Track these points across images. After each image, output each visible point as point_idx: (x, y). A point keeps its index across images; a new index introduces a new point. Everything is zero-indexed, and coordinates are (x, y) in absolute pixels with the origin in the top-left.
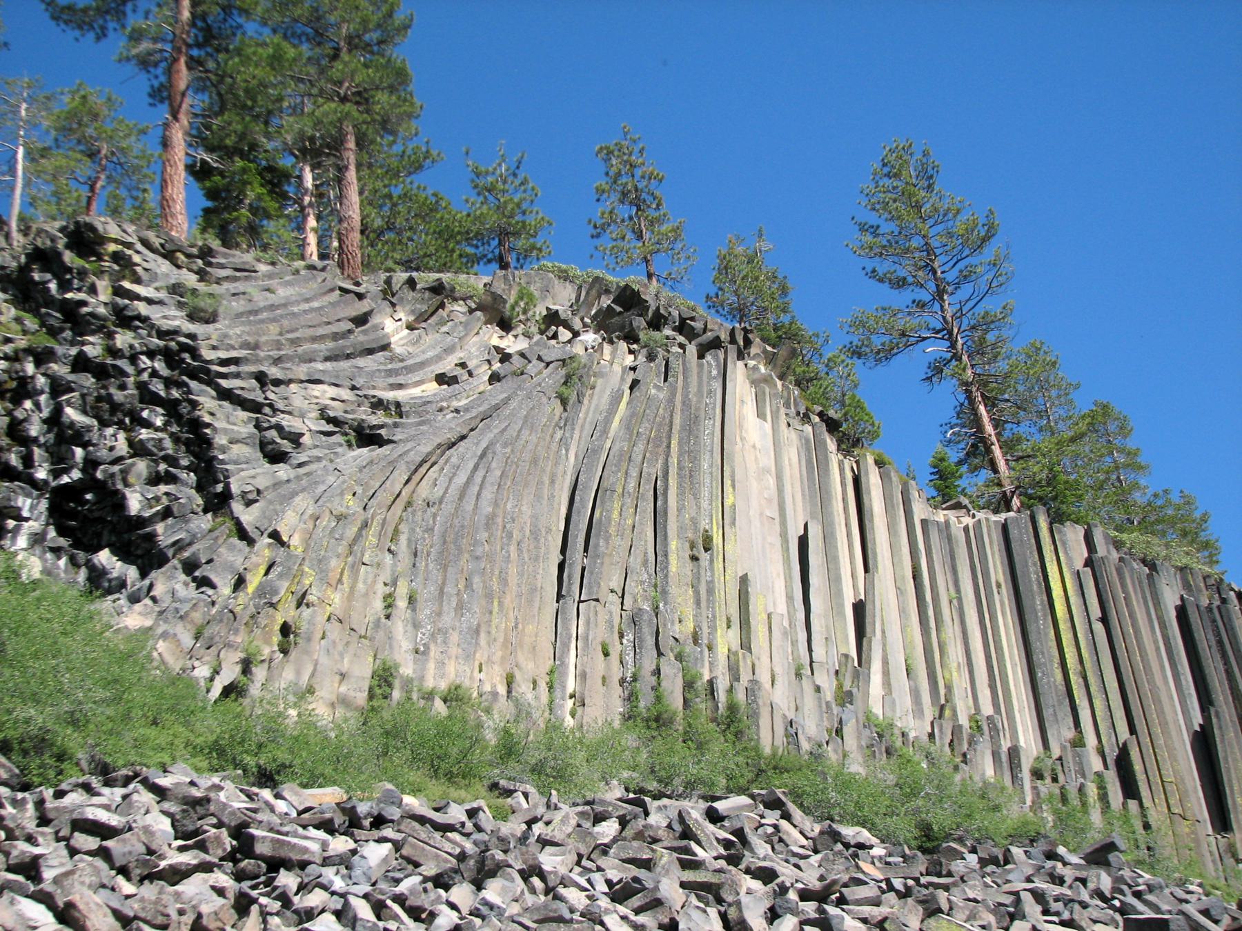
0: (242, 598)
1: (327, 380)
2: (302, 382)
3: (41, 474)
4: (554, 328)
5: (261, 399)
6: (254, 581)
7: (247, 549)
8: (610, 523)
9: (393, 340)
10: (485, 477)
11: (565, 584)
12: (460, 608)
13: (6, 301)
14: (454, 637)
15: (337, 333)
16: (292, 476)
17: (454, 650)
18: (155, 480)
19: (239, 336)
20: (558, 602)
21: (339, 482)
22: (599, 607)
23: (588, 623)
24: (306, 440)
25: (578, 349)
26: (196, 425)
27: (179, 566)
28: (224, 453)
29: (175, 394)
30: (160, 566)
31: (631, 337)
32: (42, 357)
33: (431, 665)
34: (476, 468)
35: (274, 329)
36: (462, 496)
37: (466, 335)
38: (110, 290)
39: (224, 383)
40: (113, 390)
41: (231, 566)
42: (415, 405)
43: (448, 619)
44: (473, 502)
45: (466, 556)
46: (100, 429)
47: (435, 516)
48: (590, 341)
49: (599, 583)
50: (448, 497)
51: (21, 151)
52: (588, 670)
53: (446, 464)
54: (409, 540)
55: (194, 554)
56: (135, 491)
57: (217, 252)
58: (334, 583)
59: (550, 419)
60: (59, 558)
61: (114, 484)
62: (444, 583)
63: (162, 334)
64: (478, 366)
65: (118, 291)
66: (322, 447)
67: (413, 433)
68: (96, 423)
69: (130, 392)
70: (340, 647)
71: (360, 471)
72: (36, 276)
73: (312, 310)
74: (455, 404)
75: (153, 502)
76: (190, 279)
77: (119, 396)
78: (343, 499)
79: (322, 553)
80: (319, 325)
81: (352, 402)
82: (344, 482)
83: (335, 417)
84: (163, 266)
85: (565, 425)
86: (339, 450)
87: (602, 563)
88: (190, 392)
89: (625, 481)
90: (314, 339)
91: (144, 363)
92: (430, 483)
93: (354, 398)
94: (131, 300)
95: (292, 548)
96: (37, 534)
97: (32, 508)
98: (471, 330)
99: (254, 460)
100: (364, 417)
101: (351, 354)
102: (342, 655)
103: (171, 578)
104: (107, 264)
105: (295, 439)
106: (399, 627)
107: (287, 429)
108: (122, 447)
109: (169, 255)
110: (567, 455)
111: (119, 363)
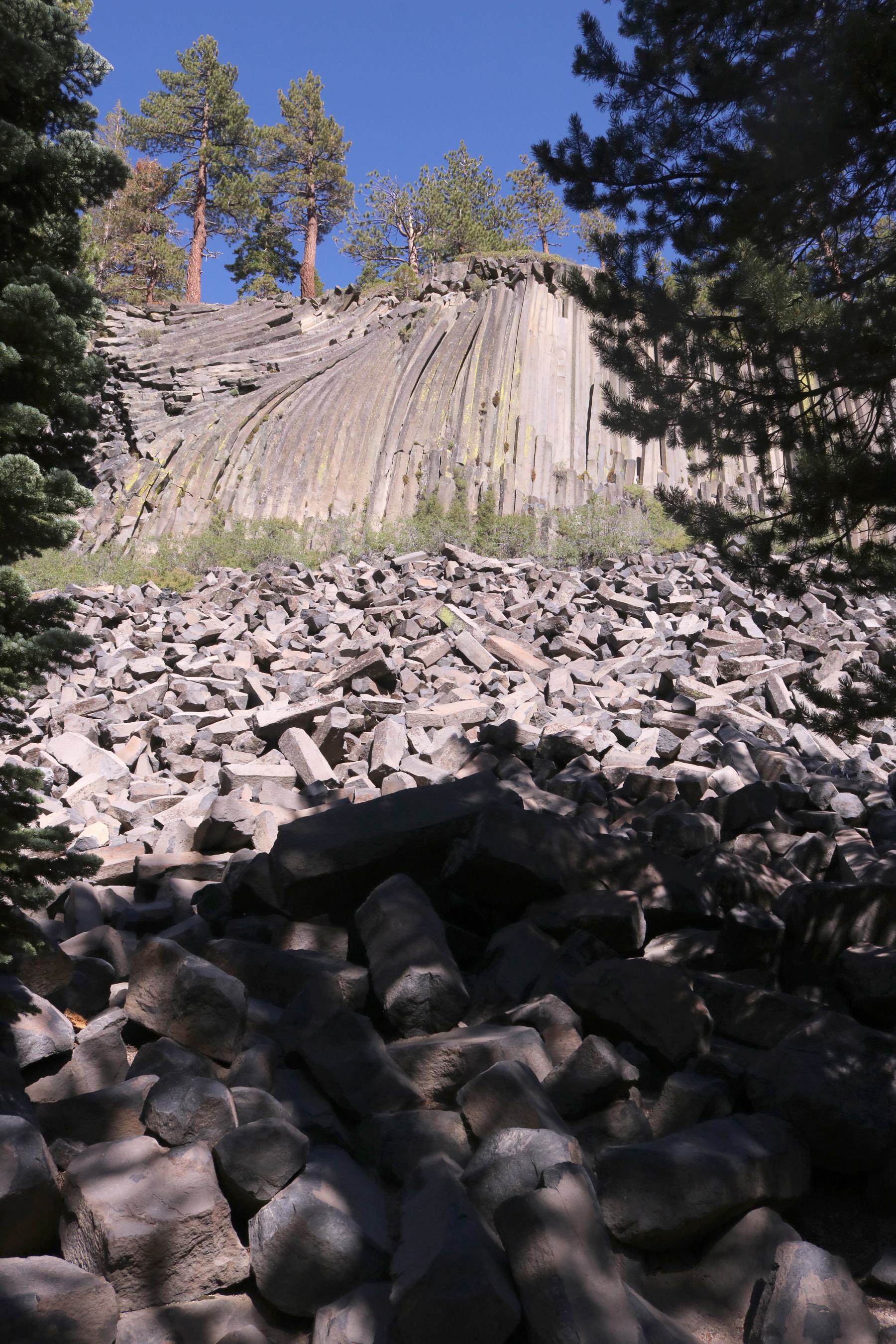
14: (288, 490)
34: (322, 390)
36: (307, 408)
39: (144, 379)
47: (283, 424)
58: (186, 475)
90: (229, 340)
102: (191, 514)
105: (188, 399)
106: (244, 491)
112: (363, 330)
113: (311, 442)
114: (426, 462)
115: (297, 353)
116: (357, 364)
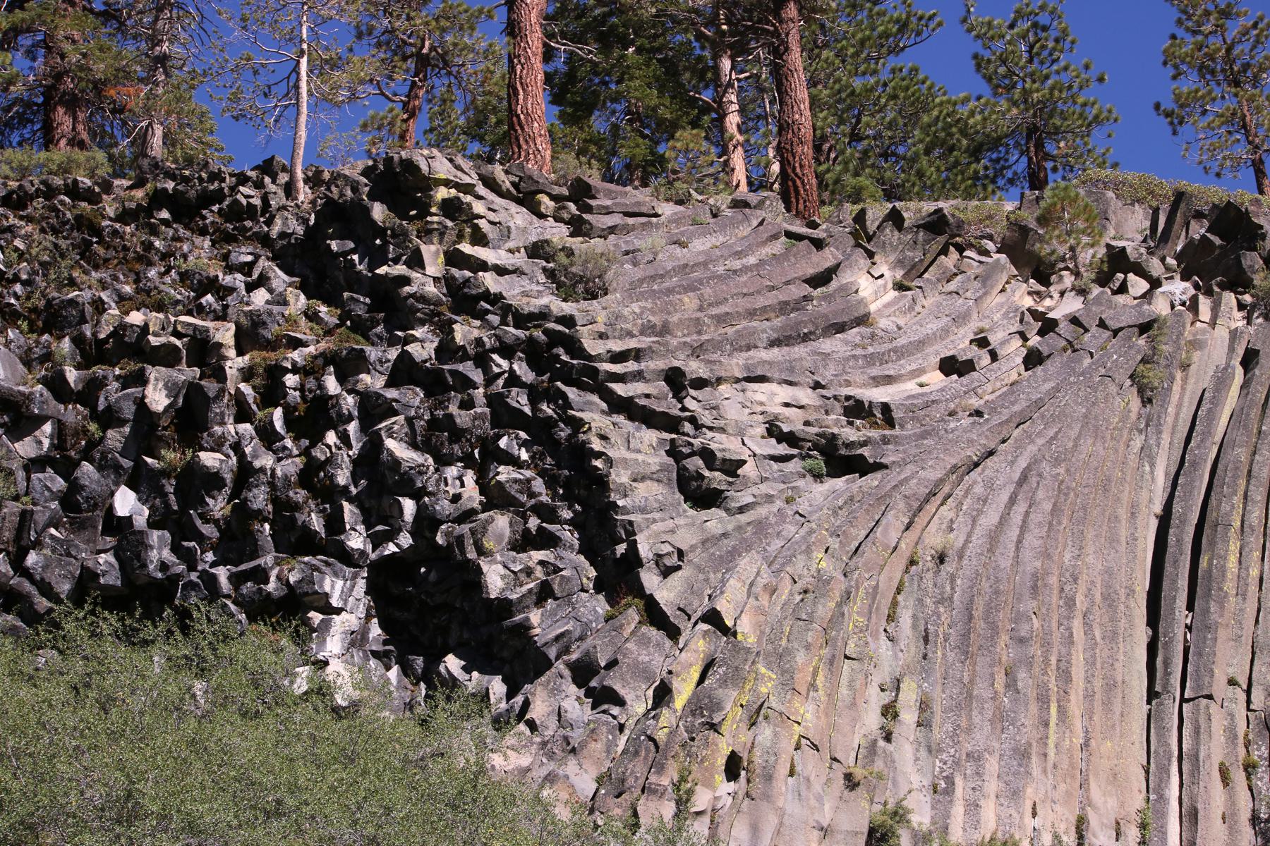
0: (667, 717)
1: (776, 376)
2: (738, 380)
3: (356, 541)
4: (1120, 276)
5: (676, 412)
6: (683, 692)
7: (668, 643)
8: (1224, 576)
9: (873, 308)
10: (1027, 514)
11: (1159, 674)
12: (1001, 720)
13: (290, 285)
14: (992, 765)
15: (787, 303)
16: (730, 527)
17: (992, 786)
18: (524, 542)
19: (640, 316)
20: (1149, 702)
21: (803, 532)
22: (1214, 708)
23: (1197, 731)
24: (748, 470)
25: (1160, 307)
26: (579, 455)
27: (567, 673)
28: (626, 496)
29: (547, 409)
30: (539, 674)
31: (1238, 282)
32: (349, 366)
33: (958, 810)
34: (1012, 500)
35: (689, 302)
37: (985, 294)
38: (441, 259)
39: (619, 389)
40: (453, 409)
41: (645, 671)
42: (911, 410)
43: (981, 738)
44: (1012, 554)
45: (1004, 638)
46: (437, 470)
47: (953, 579)
48: (1178, 292)
49: (1212, 670)
50: (971, 550)
51: (304, 61)
52: (1200, 806)
53: (967, 492)
54: (914, 617)
55: (587, 653)
56: (494, 562)
57: (598, 191)
58: (804, 693)
59: (1125, 417)
60: (388, 668)
61: (463, 552)
62: (972, 682)
63: (522, 320)
64: (1004, 343)
65: (454, 258)
66: (774, 480)
67: (913, 451)
68: (431, 461)
69: (479, 410)
70: (817, 787)
71: (835, 513)
72: (334, 245)
73: (746, 269)
74: (975, 403)
75: (522, 577)
76: (557, 233)
77: (463, 418)
78: (810, 559)
79: (784, 642)
80: (759, 292)
81: (817, 408)
82: (811, 532)
83: (791, 433)
84: (518, 217)
85: (1147, 425)
86: (801, 483)
88: (568, 405)
89: (1244, 509)
90: (751, 314)
91: (498, 366)
92: (944, 526)
93: (818, 402)
94: (475, 272)
95: (739, 637)
96: (353, 633)
97: (345, 596)
98: (992, 287)
99: (672, 505)
100: (835, 430)
101: (811, 333)
102: (819, 799)
103: (555, 691)
104: (435, 219)
105: (732, 467)
106: (905, 750)
107: (719, 455)
108: (471, 493)
109: (526, 197)
110: (1152, 472)
111: (460, 367)
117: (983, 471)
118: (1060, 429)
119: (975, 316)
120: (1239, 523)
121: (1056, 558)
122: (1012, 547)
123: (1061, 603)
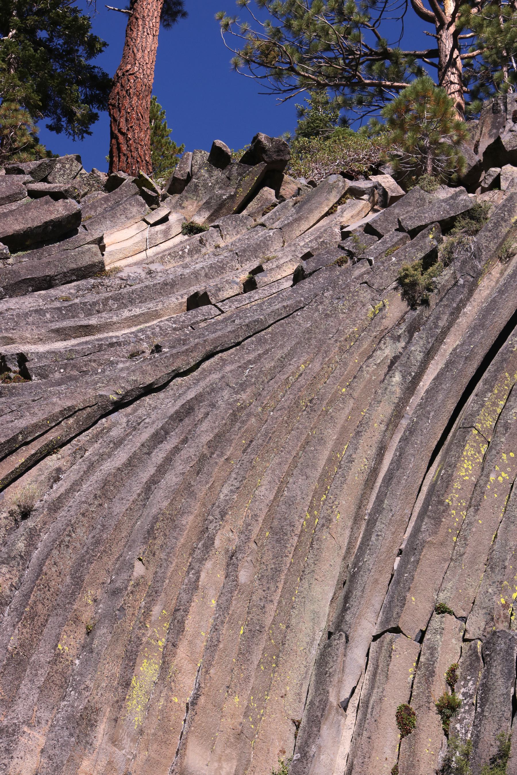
10: (177, 450)
23: (375, 674)
37: (298, 220)
49: (405, 598)
53: (96, 438)
87: (418, 562)
98: (311, 211)
112: (290, 269)
113: (115, 593)
114: (472, 668)
115: (88, 330)
116: (268, 364)
117: (135, 410)
118: (266, 352)
119: (277, 245)
120: (490, 423)
121: (201, 495)
122: (137, 489)
123: (200, 545)
